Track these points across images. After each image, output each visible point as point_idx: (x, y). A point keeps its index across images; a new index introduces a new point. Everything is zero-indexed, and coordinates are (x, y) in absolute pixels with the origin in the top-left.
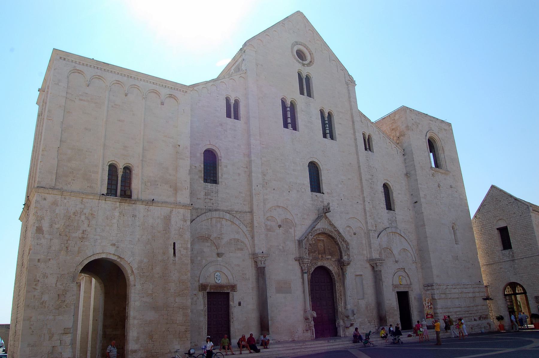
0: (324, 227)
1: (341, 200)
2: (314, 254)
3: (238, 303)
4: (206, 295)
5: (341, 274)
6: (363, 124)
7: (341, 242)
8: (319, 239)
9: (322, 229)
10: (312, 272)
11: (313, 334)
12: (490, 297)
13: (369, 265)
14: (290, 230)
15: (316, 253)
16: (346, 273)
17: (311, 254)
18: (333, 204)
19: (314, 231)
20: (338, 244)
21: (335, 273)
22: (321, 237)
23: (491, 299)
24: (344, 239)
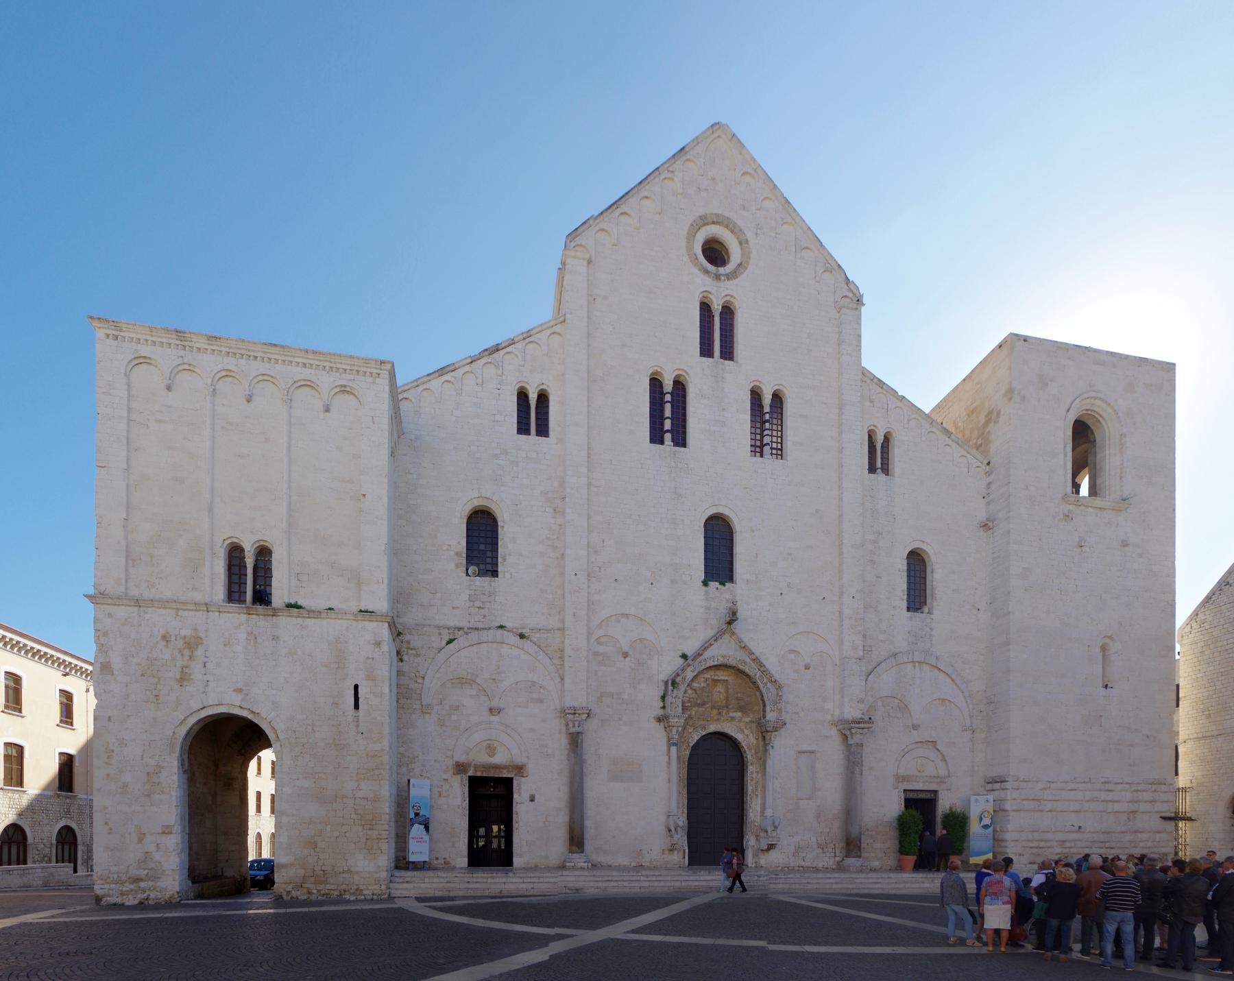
2: (701, 709)
3: (528, 796)
4: (466, 782)
6: (873, 406)
7: (766, 684)
8: (716, 678)
9: (719, 658)
12: (1188, 815)
13: (836, 732)
15: (708, 705)
17: (694, 709)
19: (700, 662)
20: (758, 688)
22: (722, 675)
23: (1190, 819)
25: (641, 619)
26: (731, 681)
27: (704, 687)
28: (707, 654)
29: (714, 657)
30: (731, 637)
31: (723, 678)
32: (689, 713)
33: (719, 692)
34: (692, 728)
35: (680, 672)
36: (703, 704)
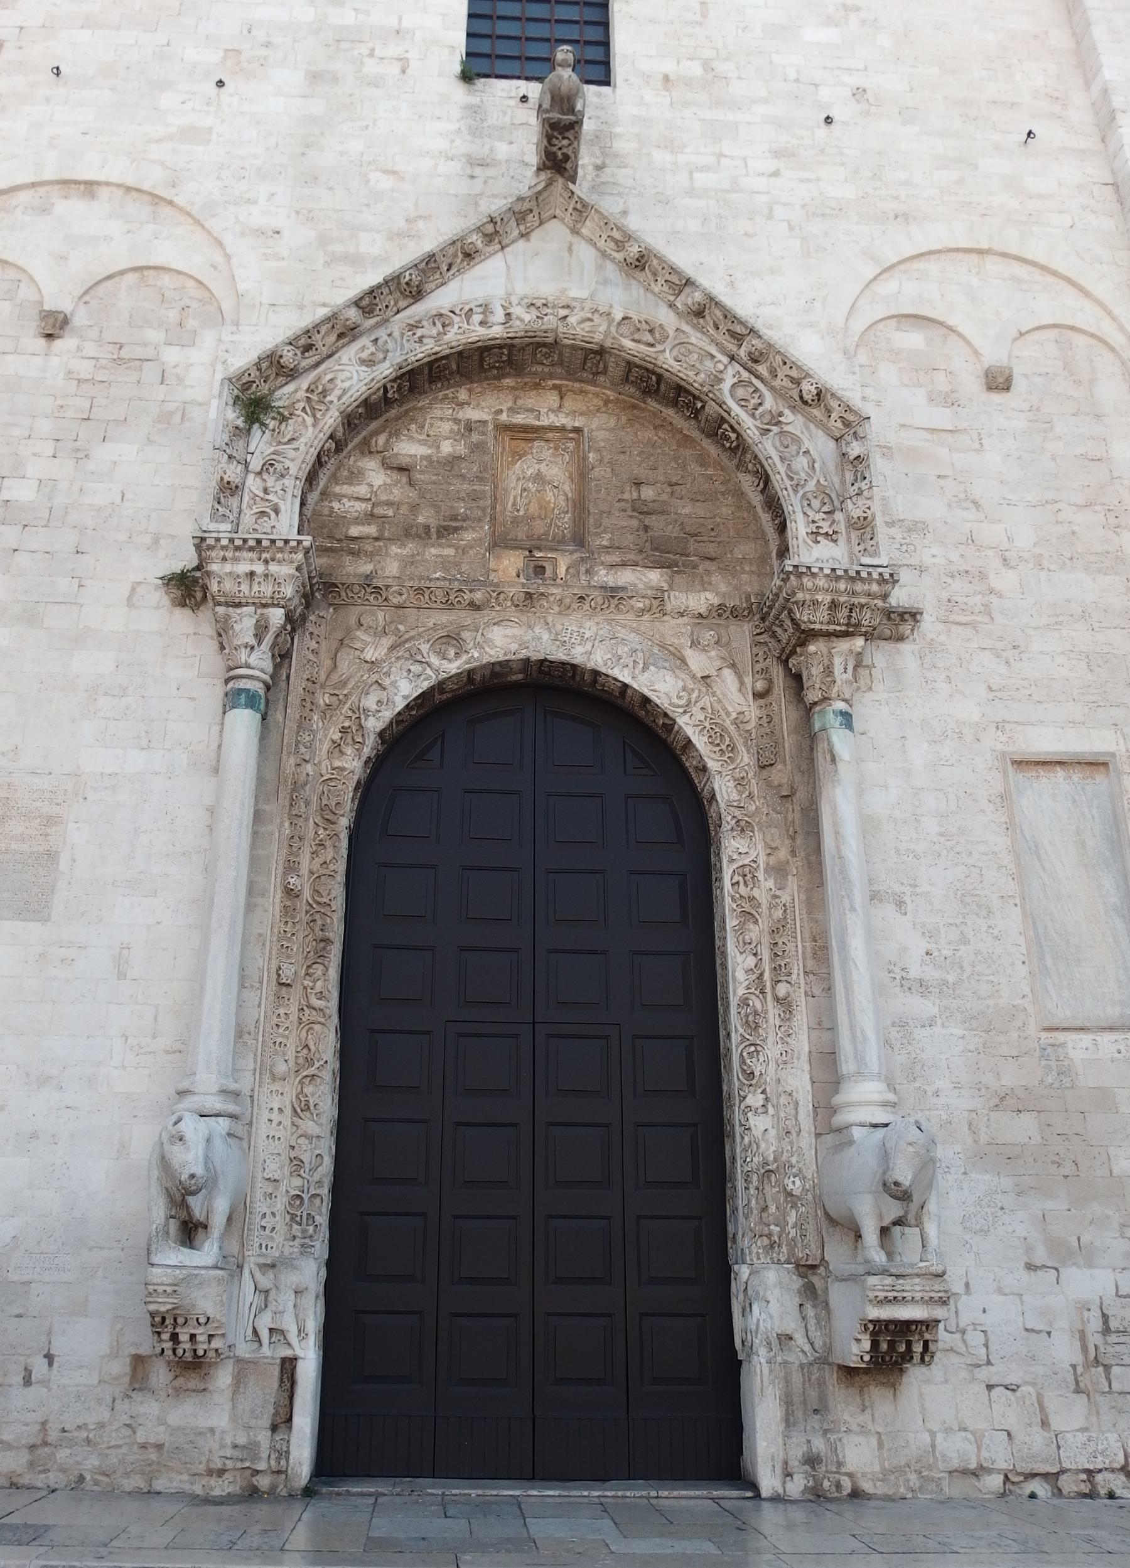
0: (548, 289)
1: (828, 120)
2: (433, 551)
5: (789, 742)
8: (520, 419)
9: (518, 311)
10: (388, 715)
11: (283, 1421)
14: (171, 355)
15: (469, 536)
16: (833, 721)
17: (394, 549)
18: (721, 155)
19: (413, 327)
21: (717, 735)
24: (797, 382)
25: (156, 199)
26: (601, 435)
27: (454, 460)
28: (441, 299)
29: (486, 309)
30: (575, 232)
31: (561, 420)
32: (368, 568)
33: (539, 478)
34: (387, 642)
35: (289, 357)
36: (446, 531)
